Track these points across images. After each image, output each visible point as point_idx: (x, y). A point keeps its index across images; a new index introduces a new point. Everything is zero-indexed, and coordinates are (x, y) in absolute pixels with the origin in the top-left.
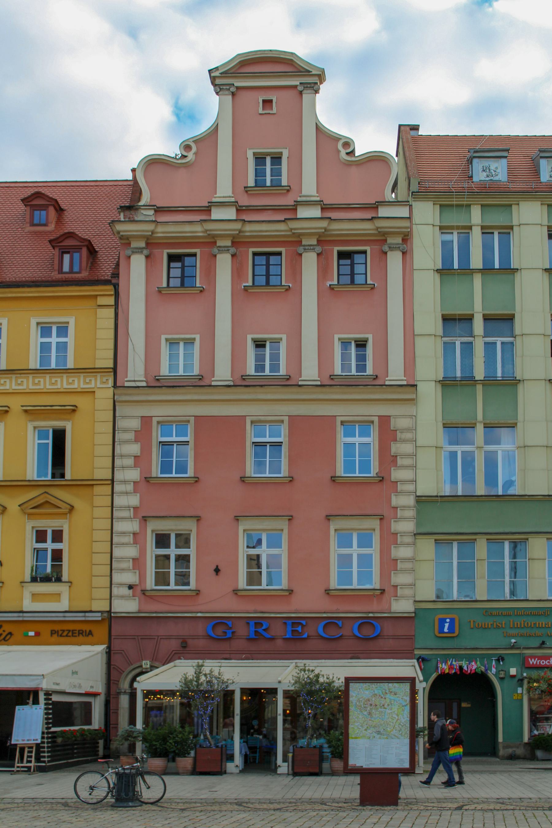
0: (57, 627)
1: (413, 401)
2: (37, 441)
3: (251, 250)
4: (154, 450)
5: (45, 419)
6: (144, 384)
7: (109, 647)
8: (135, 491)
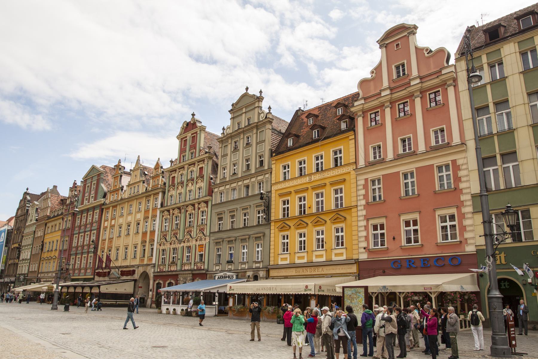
1: (465, 151)
3: (428, 93)
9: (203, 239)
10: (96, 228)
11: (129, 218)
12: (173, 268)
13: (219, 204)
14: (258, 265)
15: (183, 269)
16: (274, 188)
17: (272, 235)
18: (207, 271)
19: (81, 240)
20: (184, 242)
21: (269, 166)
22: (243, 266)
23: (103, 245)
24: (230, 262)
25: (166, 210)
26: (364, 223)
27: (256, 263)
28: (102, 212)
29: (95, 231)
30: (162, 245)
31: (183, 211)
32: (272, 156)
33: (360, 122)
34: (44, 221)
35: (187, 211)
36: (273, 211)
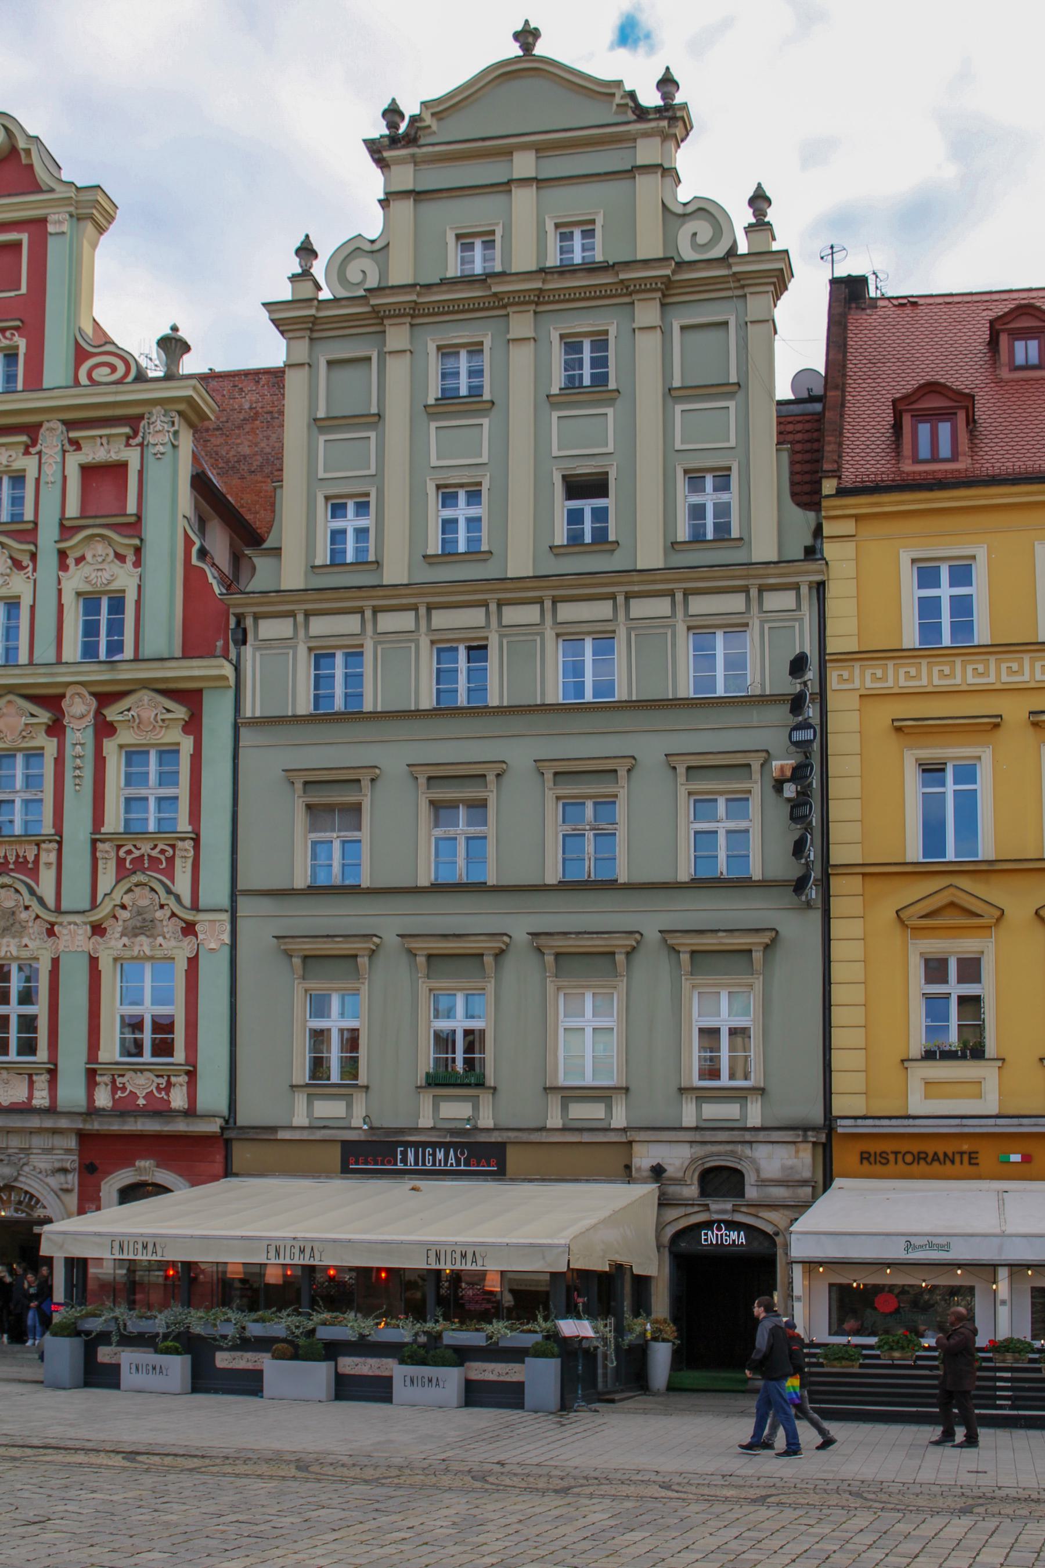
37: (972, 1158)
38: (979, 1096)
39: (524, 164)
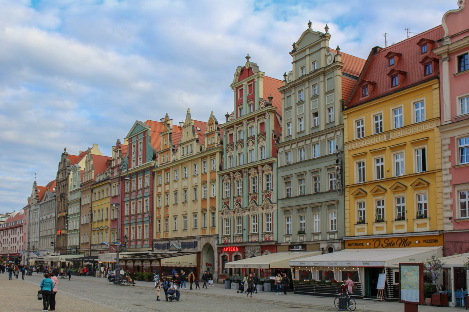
0: (426, 239)
2: (417, 156)
4: (456, 152)
5: (418, 146)
6: (450, 122)
7: (444, 247)
8: (450, 173)
9: (270, 207)
10: (148, 194)
11: (185, 183)
12: (238, 240)
13: (286, 166)
14: (332, 236)
15: (250, 241)
16: (347, 148)
17: (347, 203)
18: (277, 242)
19: (133, 207)
20: (249, 210)
21: (340, 121)
22: (316, 237)
23: (159, 214)
24: (301, 233)
25: (225, 173)
26: (449, 190)
27: (330, 234)
28: (154, 176)
29: (148, 198)
30: (224, 213)
31: (245, 174)
32: (343, 109)
33: (445, 67)
34: (89, 187)
35: (249, 175)
36: (346, 174)
37: (362, 244)
38: (364, 231)
39: (308, 52)
